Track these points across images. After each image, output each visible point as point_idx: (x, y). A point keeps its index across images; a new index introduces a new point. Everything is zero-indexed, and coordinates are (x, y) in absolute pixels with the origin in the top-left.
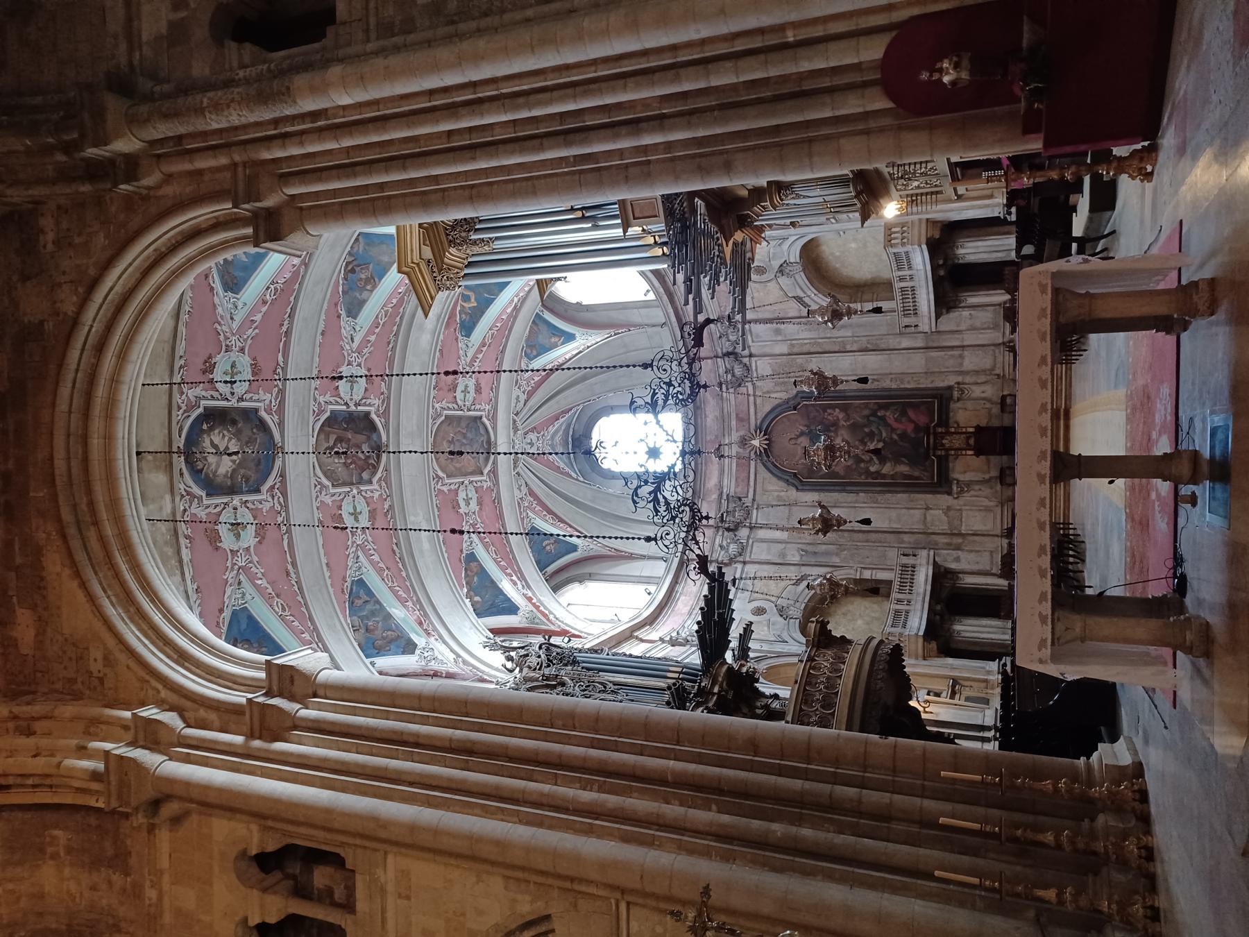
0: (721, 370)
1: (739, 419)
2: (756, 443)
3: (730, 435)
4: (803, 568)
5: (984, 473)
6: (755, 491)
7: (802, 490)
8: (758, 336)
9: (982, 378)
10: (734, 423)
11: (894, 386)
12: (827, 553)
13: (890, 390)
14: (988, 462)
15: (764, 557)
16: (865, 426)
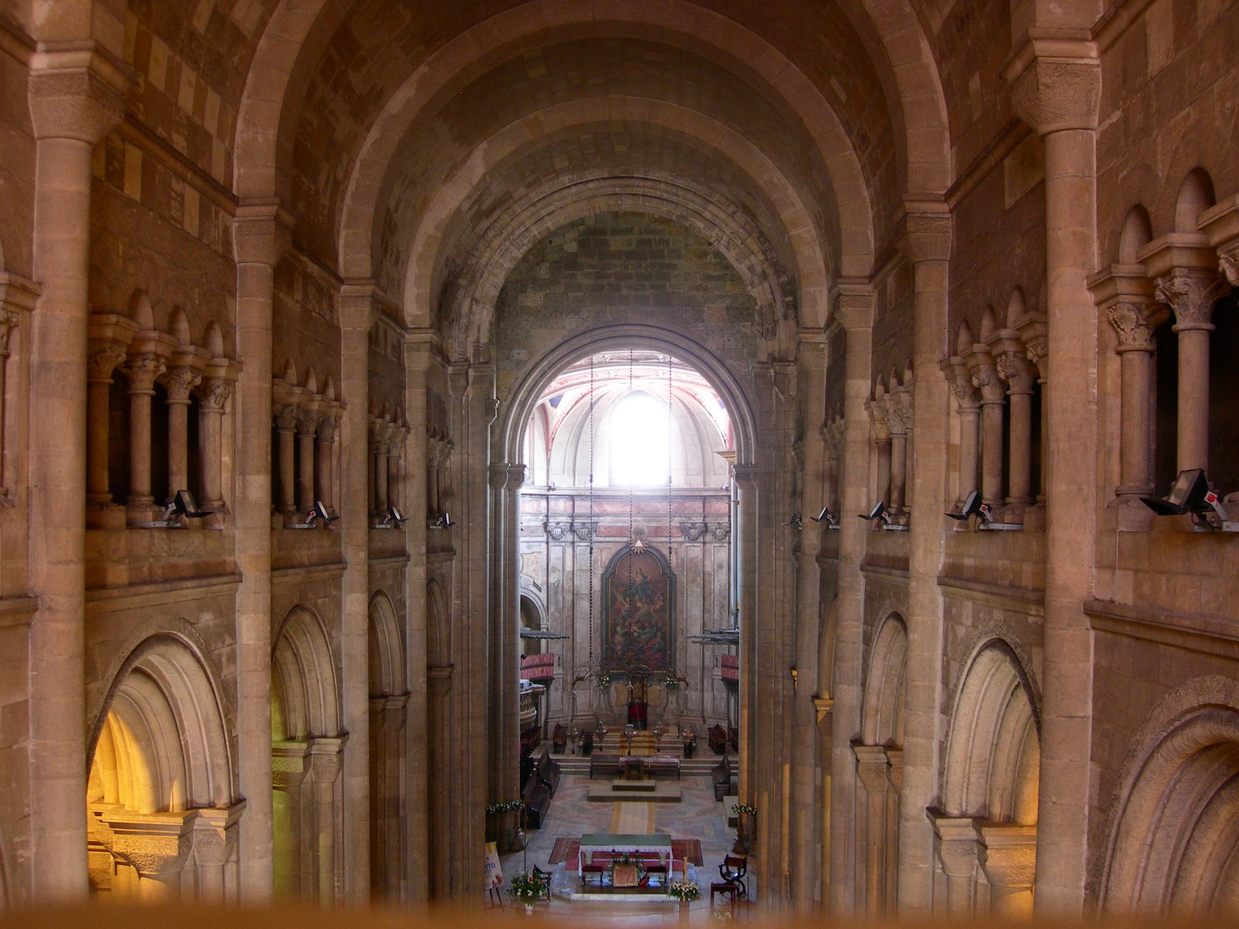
0: (694, 519)
1: (657, 528)
2: (639, 544)
3: (645, 521)
4: (545, 586)
5: (616, 703)
6: (601, 542)
7: (602, 579)
8: (718, 551)
9: (681, 702)
10: (654, 524)
11: (678, 644)
12: (557, 603)
13: (676, 641)
14: (623, 706)
15: (552, 556)
16: (650, 624)
